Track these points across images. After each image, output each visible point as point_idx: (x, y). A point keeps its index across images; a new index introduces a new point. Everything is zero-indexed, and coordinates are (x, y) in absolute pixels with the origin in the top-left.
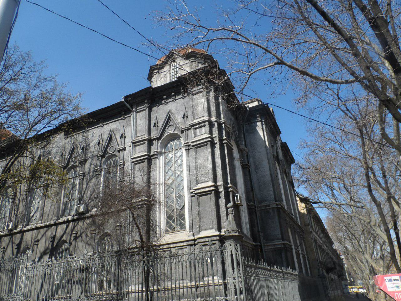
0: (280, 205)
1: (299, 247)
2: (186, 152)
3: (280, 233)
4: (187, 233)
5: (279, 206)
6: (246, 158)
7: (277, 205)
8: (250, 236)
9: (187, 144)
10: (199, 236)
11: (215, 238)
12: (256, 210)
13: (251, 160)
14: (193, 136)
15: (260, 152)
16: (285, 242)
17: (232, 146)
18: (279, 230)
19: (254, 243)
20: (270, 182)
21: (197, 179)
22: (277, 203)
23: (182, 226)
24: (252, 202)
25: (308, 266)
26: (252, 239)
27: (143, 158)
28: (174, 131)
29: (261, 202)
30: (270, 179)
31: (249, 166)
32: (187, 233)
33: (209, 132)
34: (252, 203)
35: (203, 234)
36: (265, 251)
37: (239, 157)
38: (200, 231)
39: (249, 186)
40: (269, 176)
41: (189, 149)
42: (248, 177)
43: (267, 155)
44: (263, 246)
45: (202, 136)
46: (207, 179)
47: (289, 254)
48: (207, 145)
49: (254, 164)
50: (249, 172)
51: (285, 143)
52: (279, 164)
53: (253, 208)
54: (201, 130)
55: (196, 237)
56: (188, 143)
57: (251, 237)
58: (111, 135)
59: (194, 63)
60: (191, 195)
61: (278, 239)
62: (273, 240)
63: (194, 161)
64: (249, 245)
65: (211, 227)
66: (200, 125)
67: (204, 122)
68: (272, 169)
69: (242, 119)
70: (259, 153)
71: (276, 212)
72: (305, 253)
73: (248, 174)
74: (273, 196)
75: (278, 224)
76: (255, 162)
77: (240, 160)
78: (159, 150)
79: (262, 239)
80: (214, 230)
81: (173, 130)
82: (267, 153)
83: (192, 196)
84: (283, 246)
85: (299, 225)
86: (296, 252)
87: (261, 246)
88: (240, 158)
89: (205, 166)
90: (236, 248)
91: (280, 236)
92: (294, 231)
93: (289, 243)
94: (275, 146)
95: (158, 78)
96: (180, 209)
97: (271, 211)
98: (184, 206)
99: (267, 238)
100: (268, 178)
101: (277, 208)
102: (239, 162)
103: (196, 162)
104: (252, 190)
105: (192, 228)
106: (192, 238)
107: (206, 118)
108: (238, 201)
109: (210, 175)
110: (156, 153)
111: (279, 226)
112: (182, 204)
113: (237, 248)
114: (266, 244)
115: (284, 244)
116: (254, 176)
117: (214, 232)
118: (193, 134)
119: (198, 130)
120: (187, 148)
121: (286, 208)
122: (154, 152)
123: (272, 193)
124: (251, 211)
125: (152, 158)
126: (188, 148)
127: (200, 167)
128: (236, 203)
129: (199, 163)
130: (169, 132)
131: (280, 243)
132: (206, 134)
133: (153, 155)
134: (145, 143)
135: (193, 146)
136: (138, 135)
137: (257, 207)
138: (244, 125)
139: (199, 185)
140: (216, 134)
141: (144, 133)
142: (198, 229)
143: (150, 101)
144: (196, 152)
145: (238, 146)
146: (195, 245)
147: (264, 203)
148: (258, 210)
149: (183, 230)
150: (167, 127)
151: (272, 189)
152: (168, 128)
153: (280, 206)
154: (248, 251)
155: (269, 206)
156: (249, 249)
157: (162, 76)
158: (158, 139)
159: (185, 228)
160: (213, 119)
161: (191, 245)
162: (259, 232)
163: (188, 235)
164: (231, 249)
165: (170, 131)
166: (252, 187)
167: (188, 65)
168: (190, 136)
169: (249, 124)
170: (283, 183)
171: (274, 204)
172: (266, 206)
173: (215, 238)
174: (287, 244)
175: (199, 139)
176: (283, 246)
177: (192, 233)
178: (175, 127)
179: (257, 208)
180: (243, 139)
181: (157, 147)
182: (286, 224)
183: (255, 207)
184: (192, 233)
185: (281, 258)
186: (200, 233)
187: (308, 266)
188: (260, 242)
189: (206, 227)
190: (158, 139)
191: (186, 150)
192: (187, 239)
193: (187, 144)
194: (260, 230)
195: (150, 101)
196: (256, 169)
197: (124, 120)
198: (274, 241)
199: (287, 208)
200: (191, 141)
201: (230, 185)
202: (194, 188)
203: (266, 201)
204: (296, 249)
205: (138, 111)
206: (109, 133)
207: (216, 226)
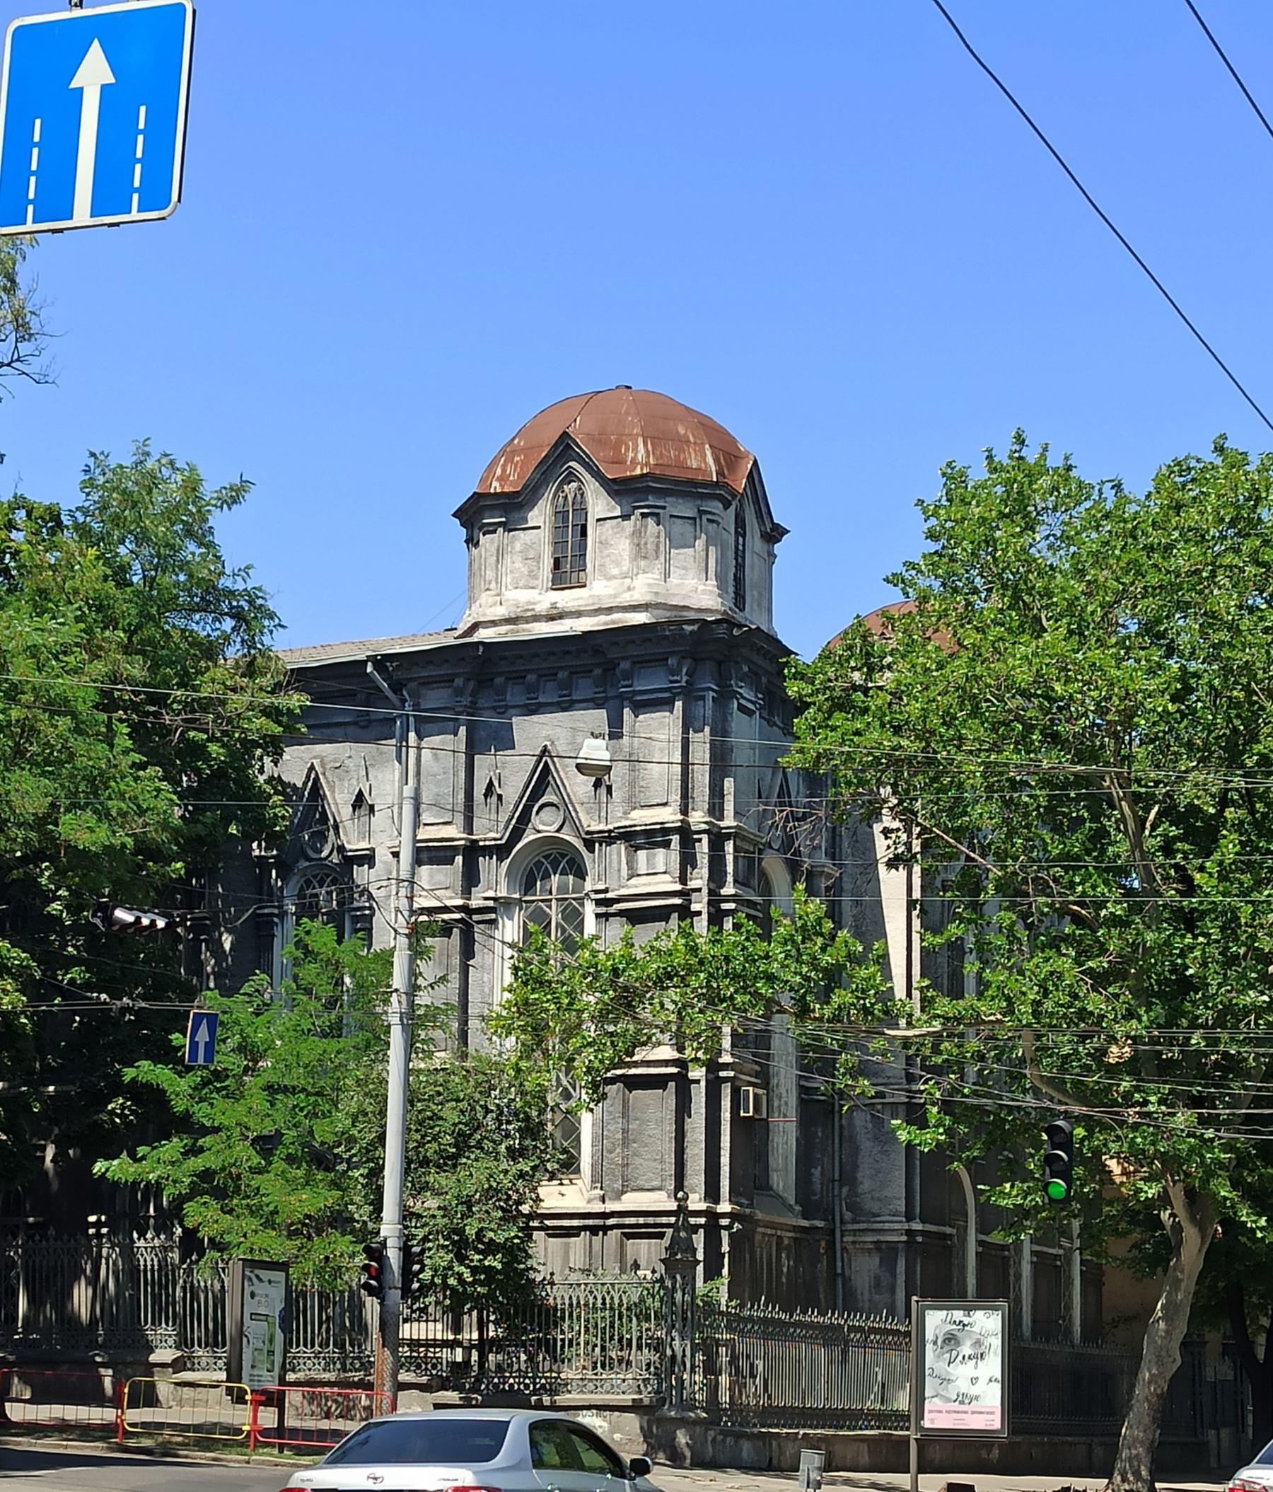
4: (584, 1190)
9: (602, 896)
11: (664, 1220)
14: (624, 872)
23: (570, 1165)
28: (558, 831)
32: (584, 1190)
35: (632, 1201)
38: (623, 1193)
54: (655, 855)
55: (611, 1206)
59: (650, 521)
65: (656, 1183)
66: (654, 837)
67: (666, 831)
78: (503, 893)
80: (662, 1195)
81: (556, 826)
95: (500, 554)
105: (597, 1179)
106: (598, 1207)
107: (670, 816)
110: (491, 903)
117: (662, 1201)
119: (642, 854)
120: (602, 910)
125: (475, 917)
130: (541, 827)
136: (426, 818)
140: (699, 879)
142: (618, 1185)
146: (606, 1229)
152: (538, 813)
157: (518, 546)
158: (501, 851)
159: (578, 1171)
160: (698, 818)
161: (594, 1230)
163: (587, 1195)
165: (545, 824)
167: (629, 525)
173: (664, 1220)
177: (599, 1192)
181: (496, 879)
184: (599, 1192)
185: (894, 1275)
186: (624, 1197)
189: (640, 1183)
190: (501, 851)
192: (583, 1207)
193: (602, 896)
201: (726, 1058)
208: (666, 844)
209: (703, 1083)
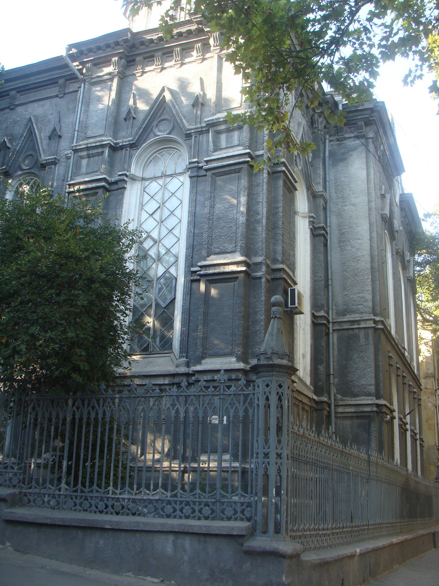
0: (382, 323)
1: (408, 417)
2: (191, 183)
3: (373, 381)
4: (174, 359)
5: (380, 326)
6: (322, 213)
7: (375, 322)
8: (308, 383)
9: (196, 165)
10: (198, 368)
12: (329, 329)
13: (333, 220)
15: (354, 205)
16: (382, 402)
17: (296, 182)
18: (373, 375)
19: (315, 397)
20: (369, 271)
21: (210, 244)
22: (377, 319)
24: (323, 312)
25: (419, 457)
26: (313, 388)
27: (94, 185)
29: (344, 313)
30: (369, 266)
31: (327, 233)
32: (174, 359)
33: (247, 143)
34: (322, 313)
35: (209, 364)
36: (336, 417)
37: (307, 211)
38: (203, 358)
39: (321, 274)
40: (368, 259)
41: (198, 176)
42: (322, 257)
43: (369, 214)
44: (333, 406)
45: (231, 150)
46: (230, 247)
47: (385, 427)
48: (239, 171)
49: (340, 230)
50: (326, 245)
51: (410, 195)
52: (392, 238)
53: (325, 324)
54: (232, 137)
56: (198, 162)
57: (311, 384)
58: (30, 128)
60: (192, 278)
61: (369, 395)
62: (356, 395)
63: (208, 203)
64: (305, 400)
68: (375, 245)
69: (325, 127)
70: (353, 208)
71: (371, 338)
72: (417, 431)
73: (322, 249)
74: (370, 304)
75: (372, 363)
76: (340, 226)
77: (310, 217)
79: (333, 390)
81: (168, 132)
82: (370, 209)
83: (193, 281)
84: (375, 409)
85: (414, 372)
86: (400, 426)
87: (329, 405)
88: (310, 211)
89: (231, 216)
90: (278, 393)
91: (372, 389)
92: (404, 384)
93: (388, 405)
94: (388, 196)
96: (164, 305)
97: (362, 334)
98: (174, 299)
99: (347, 390)
100: (365, 263)
101: (375, 329)
102: (307, 221)
103: (212, 207)
104: (327, 286)
106: (183, 370)
108: (293, 303)
109: (239, 239)
111: (373, 368)
112: (169, 298)
113: (280, 394)
114: (341, 403)
115: (378, 405)
116: (335, 256)
118: (211, 144)
121: (393, 332)
122: (120, 175)
123: (369, 297)
124: (319, 327)
126: (196, 174)
127: (219, 219)
128: (289, 306)
129: (217, 211)
130: (158, 133)
131: (369, 402)
132: (242, 148)
133: (116, 183)
134: (103, 152)
135: (207, 170)
137: (333, 323)
138: (327, 141)
139: (212, 257)
141: (101, 132)
143: (123, 61)
144: (213, 183)
145: (309, 188)
147: (348, 316)
148: (334, 330)
149: (166, 352)
150: (155, 123)
151: (370, 288)
152: (157, 125)
153: (382, 327)
154: (301, 411)
155: (358, 322)
156: (303, 409)
162: (328, 375)
163: (176, 362)
164: (267, 393)
166: (327, 280)
168: (205, 147)
169: (338, 140)
170: (394, 279)
171: (371, 320)
172: (353, 322)
174: (385, 405)
175: (224, 155)
176: (375, 409)
178: (172, 124)
179: (331, 324)
180: (321, 172)
182: (390, 365)
183: (328, 322)
185: (369, 433)
186: (203, 361)
187: (419, 457)
188: (330, 398)
191: (191, 177)
192: (172, 369)
193: (196, 165)
194: (332, 373)
195: (123, 61)
196: (340, 241)
197: (60, 98)
198: (357, 398)
199: (396, 333)
200: (205, 159)
202: (199, 264)
203: (353, 312)
204: (400, 419)
205: (93, 80)
206: (27, 125)
207: (239, 350)
208: (240, 128)
209: (263, 280)
